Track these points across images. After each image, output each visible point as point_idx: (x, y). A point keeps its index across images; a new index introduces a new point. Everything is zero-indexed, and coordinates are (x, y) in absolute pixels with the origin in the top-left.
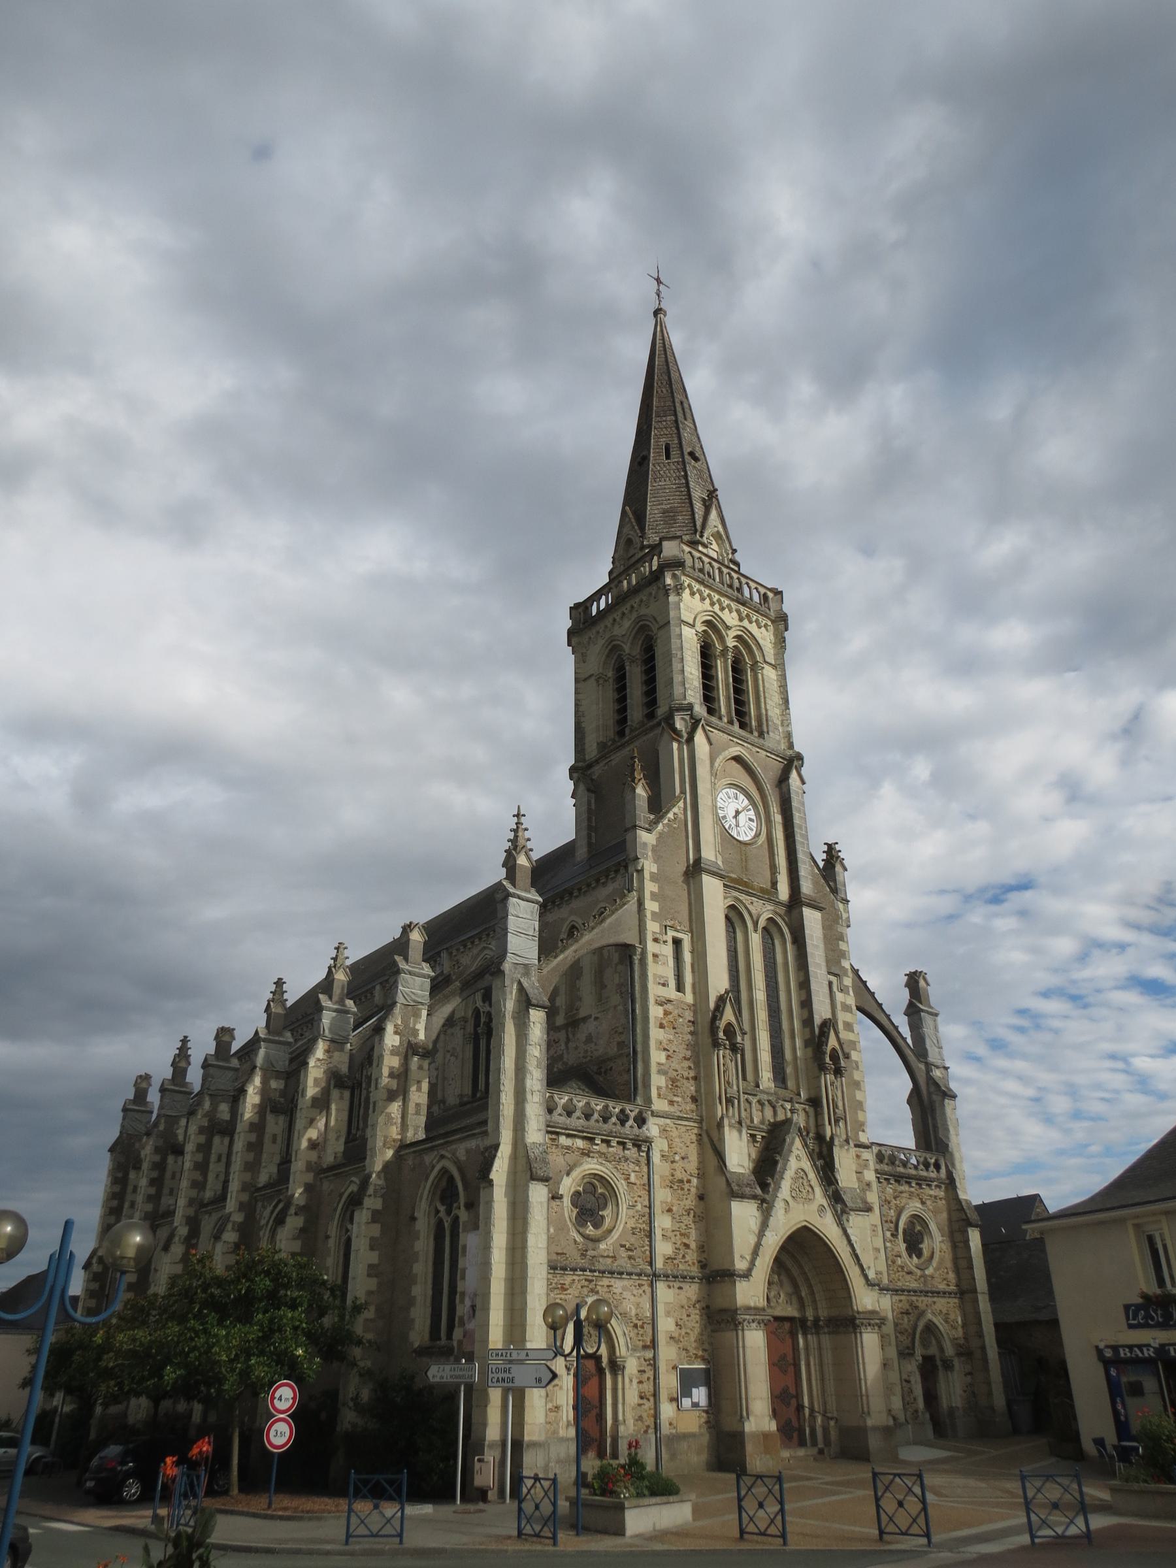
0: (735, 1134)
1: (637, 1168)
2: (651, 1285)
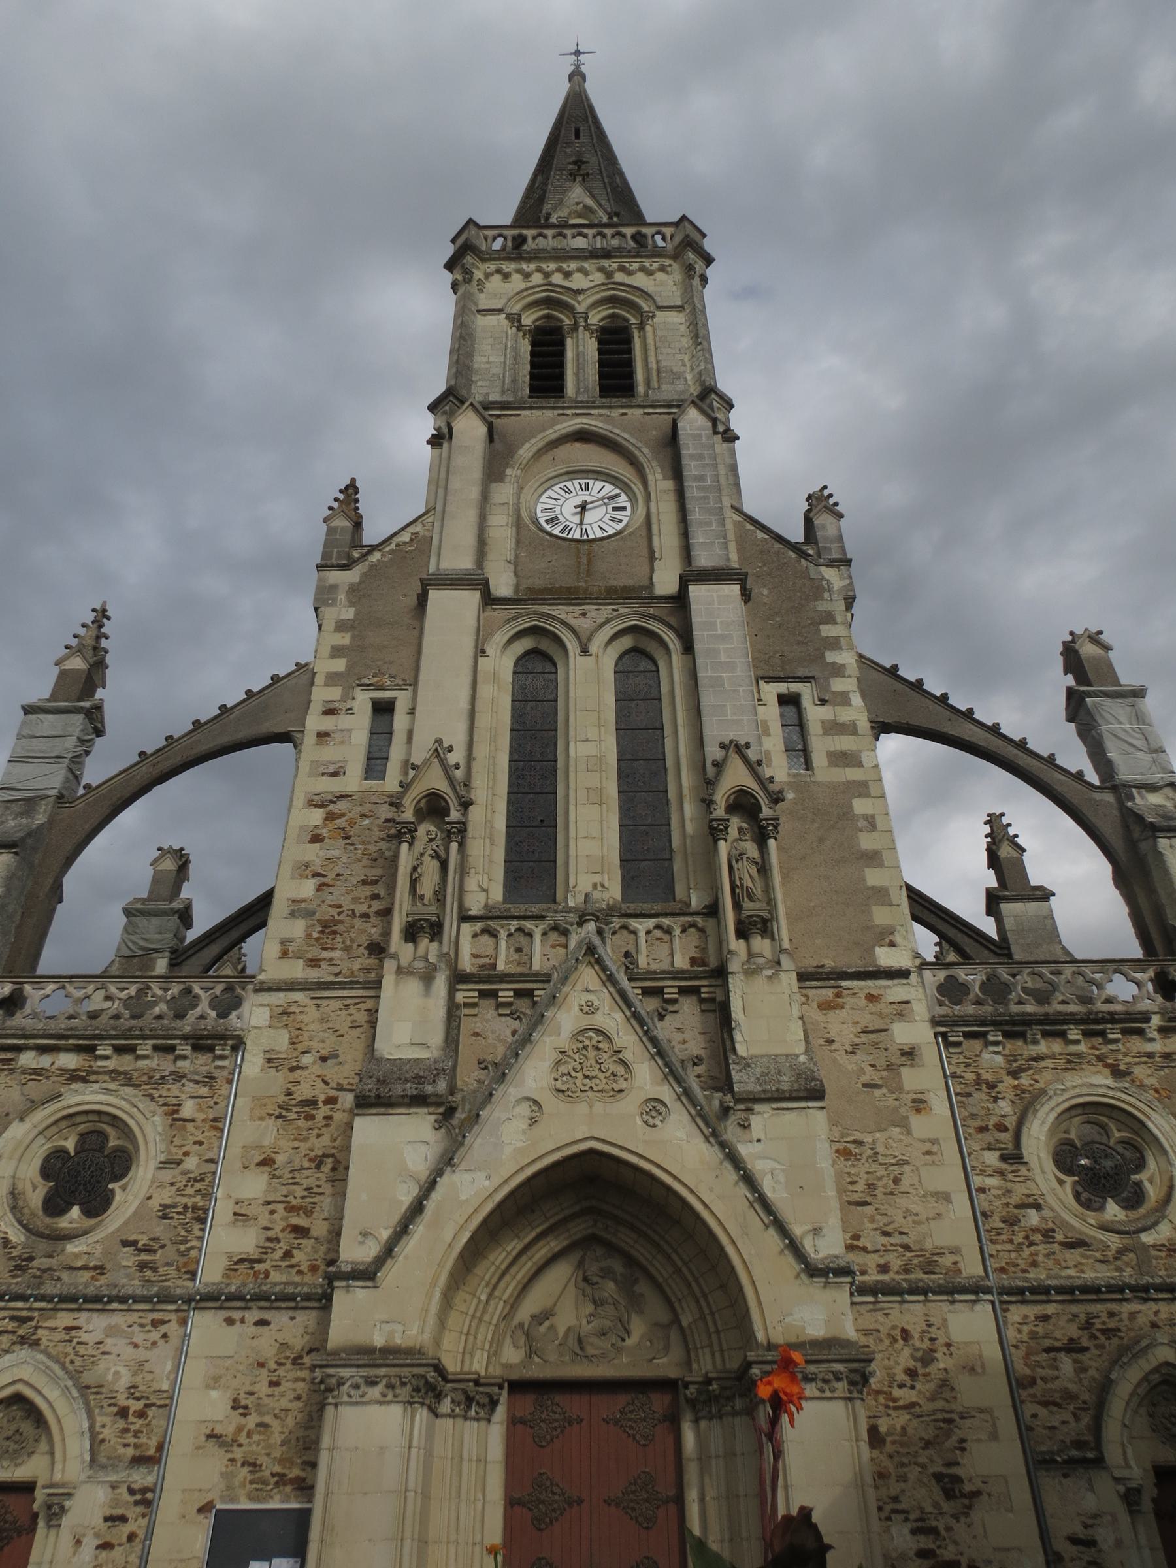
0: (413, 986)
1: (204, 1091)
2: (183, 1322)
